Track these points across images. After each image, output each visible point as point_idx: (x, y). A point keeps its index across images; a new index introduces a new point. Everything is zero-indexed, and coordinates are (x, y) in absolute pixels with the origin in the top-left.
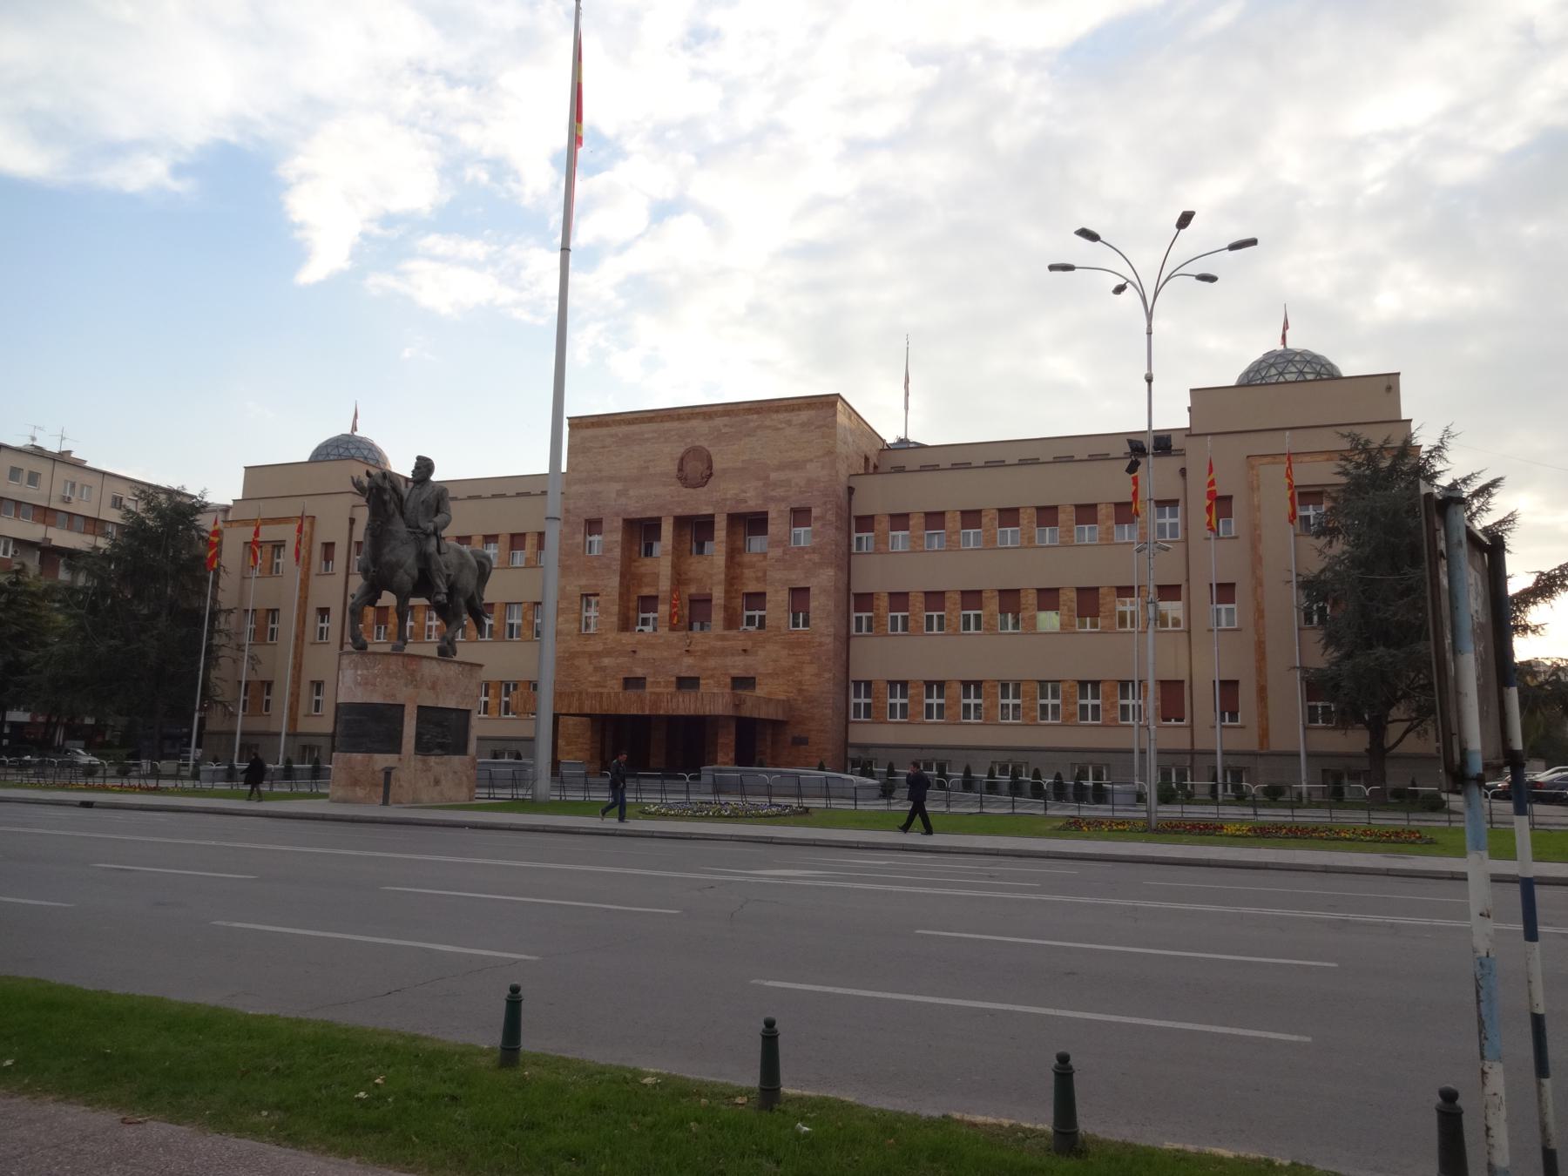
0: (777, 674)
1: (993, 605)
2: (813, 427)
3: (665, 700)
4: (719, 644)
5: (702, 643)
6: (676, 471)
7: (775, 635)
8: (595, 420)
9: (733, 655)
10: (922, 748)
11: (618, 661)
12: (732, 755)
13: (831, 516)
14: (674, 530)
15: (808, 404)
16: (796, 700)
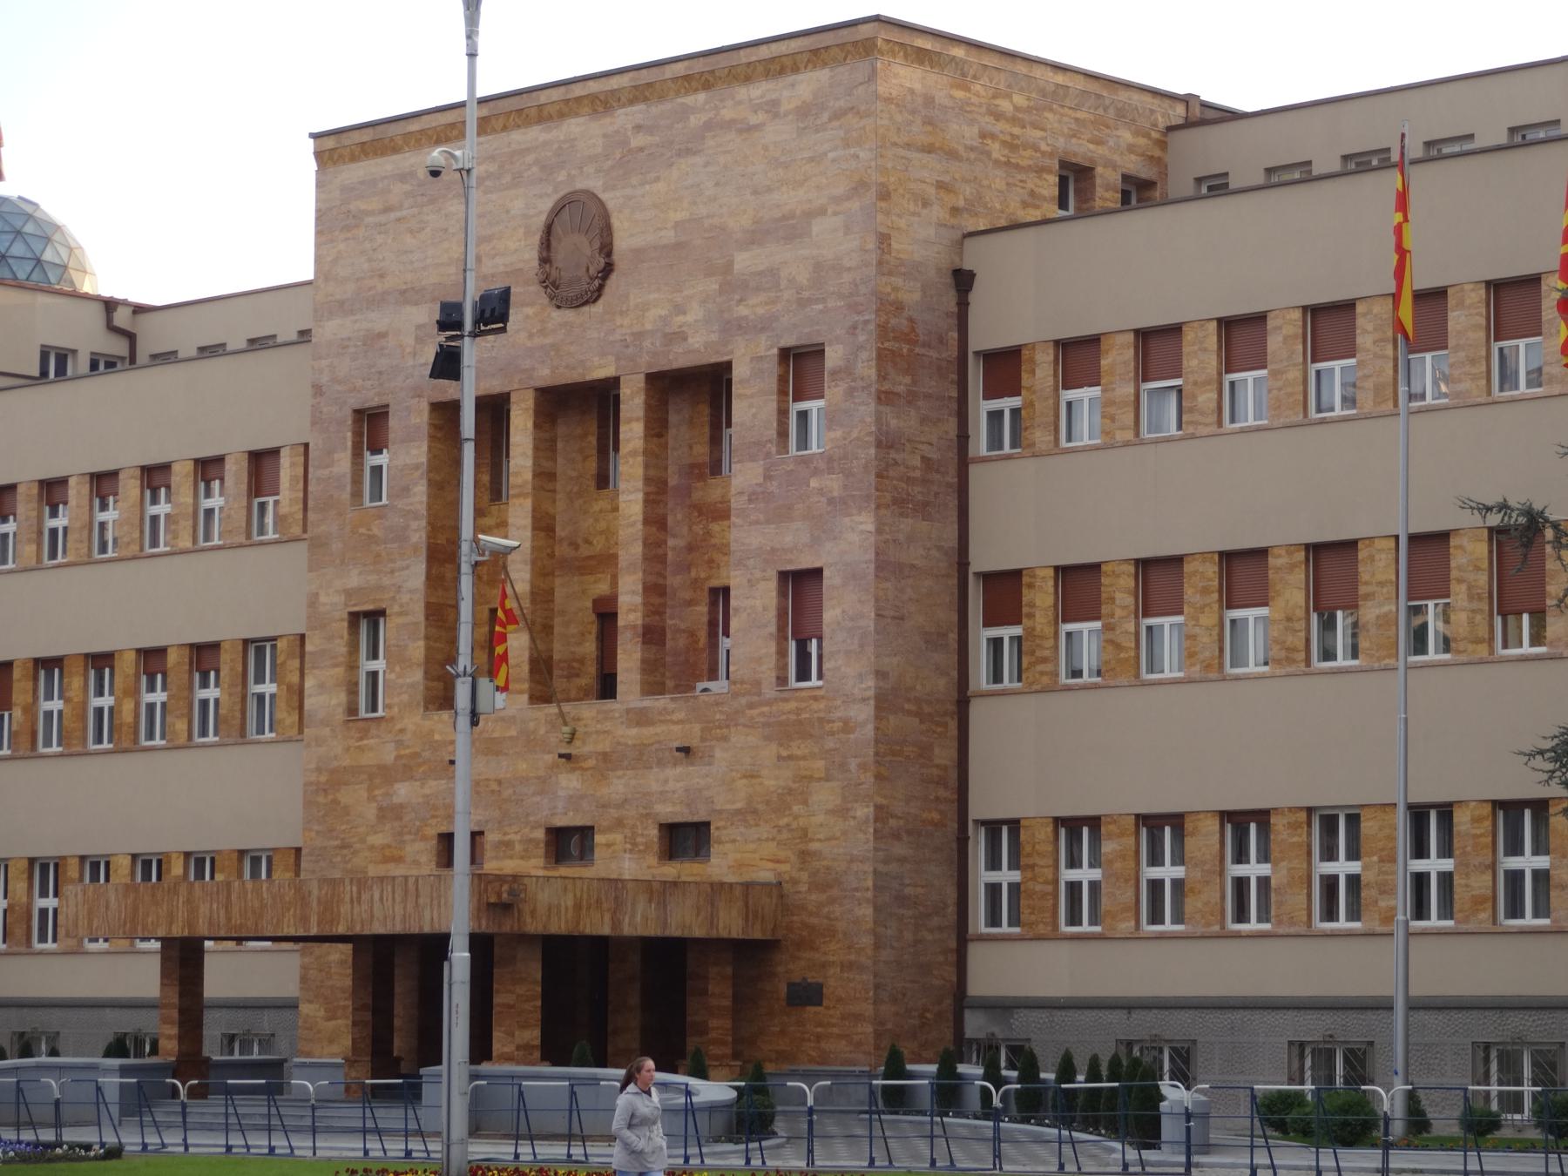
0: (755, 812)
1: (1292, 589)
2: (825, 116)
3: (347, 898)
4: (632, 734)
5: (597, 732)
6: (536, 263)
7: (751, 706)
8: (366, 136)
9: (661, 763)
10: (1129, 1006)
11: (427, 791)
12: (533, 1035)
13: (866, 368)
14: (536, 426)
15: (815, 52)
16: (794, 882)
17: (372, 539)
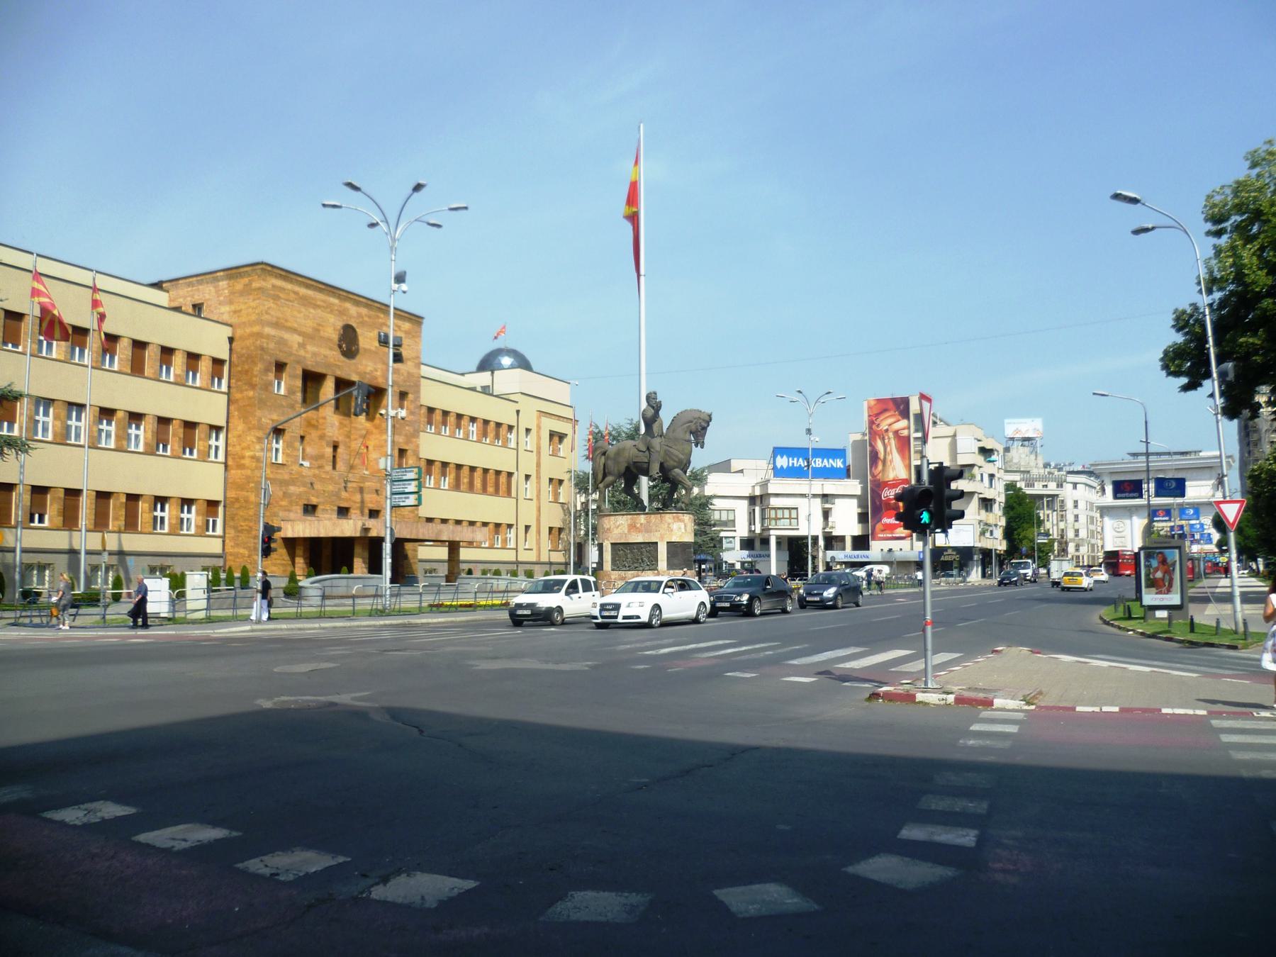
17: (282, 406)
